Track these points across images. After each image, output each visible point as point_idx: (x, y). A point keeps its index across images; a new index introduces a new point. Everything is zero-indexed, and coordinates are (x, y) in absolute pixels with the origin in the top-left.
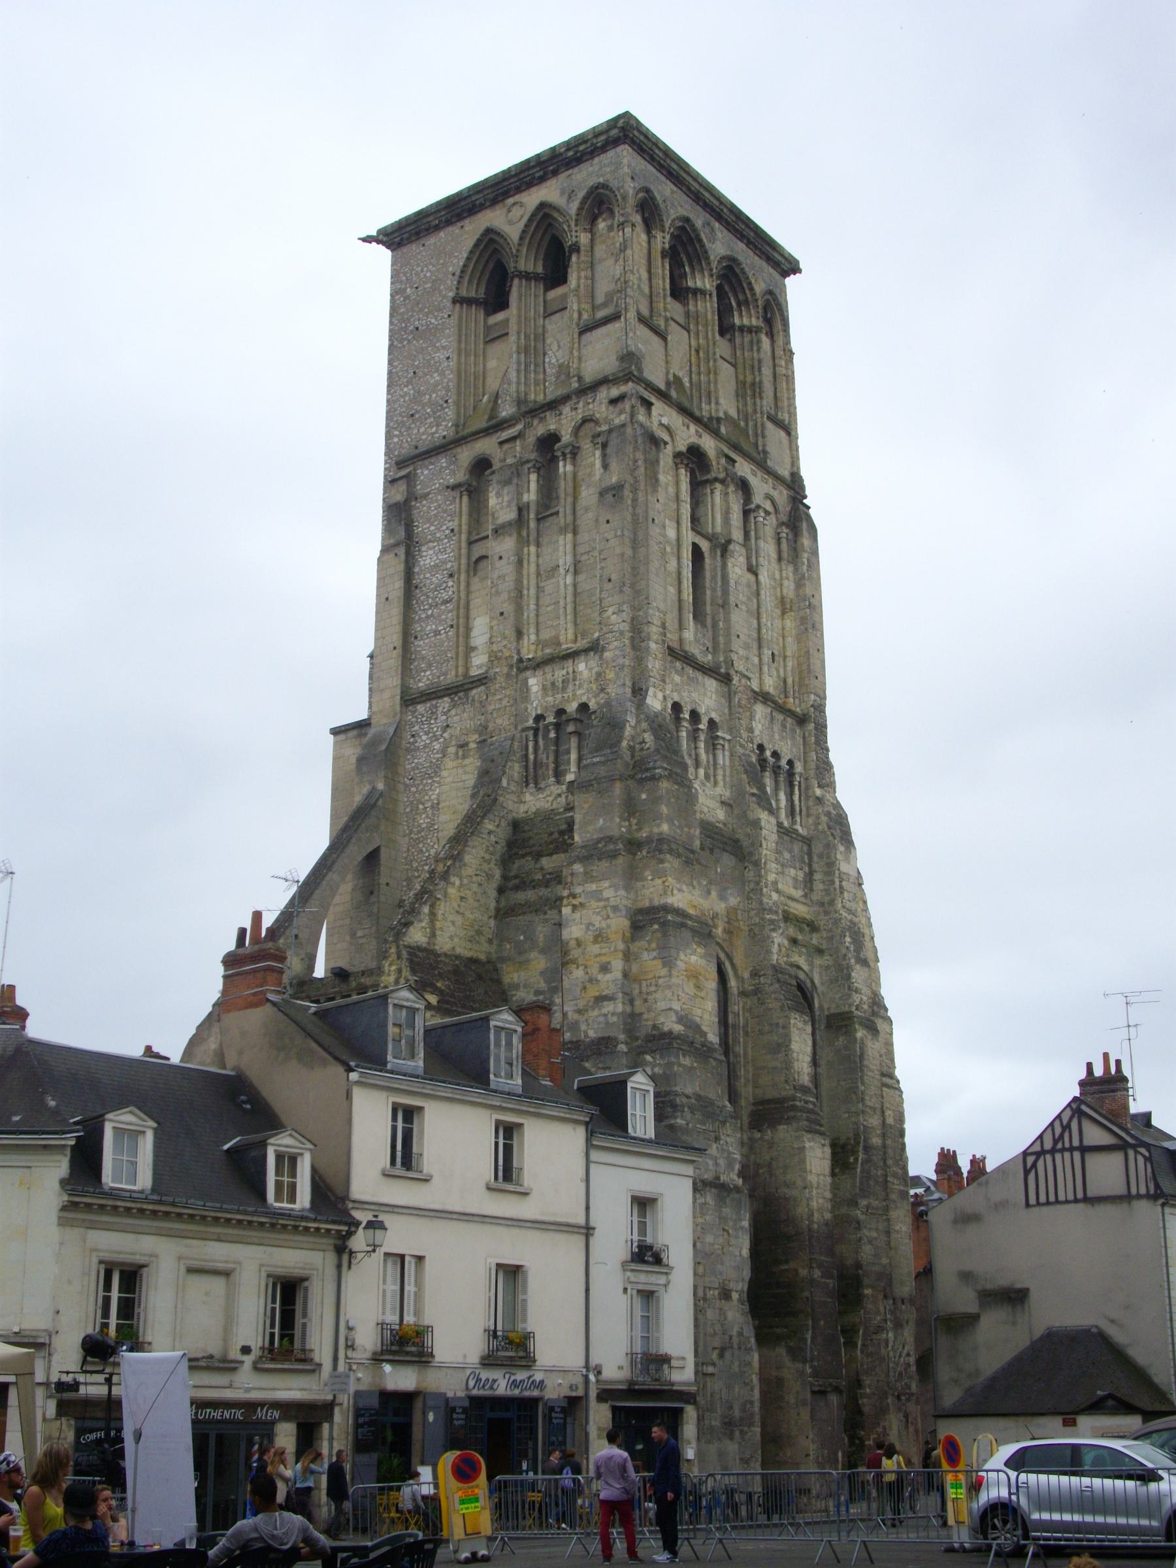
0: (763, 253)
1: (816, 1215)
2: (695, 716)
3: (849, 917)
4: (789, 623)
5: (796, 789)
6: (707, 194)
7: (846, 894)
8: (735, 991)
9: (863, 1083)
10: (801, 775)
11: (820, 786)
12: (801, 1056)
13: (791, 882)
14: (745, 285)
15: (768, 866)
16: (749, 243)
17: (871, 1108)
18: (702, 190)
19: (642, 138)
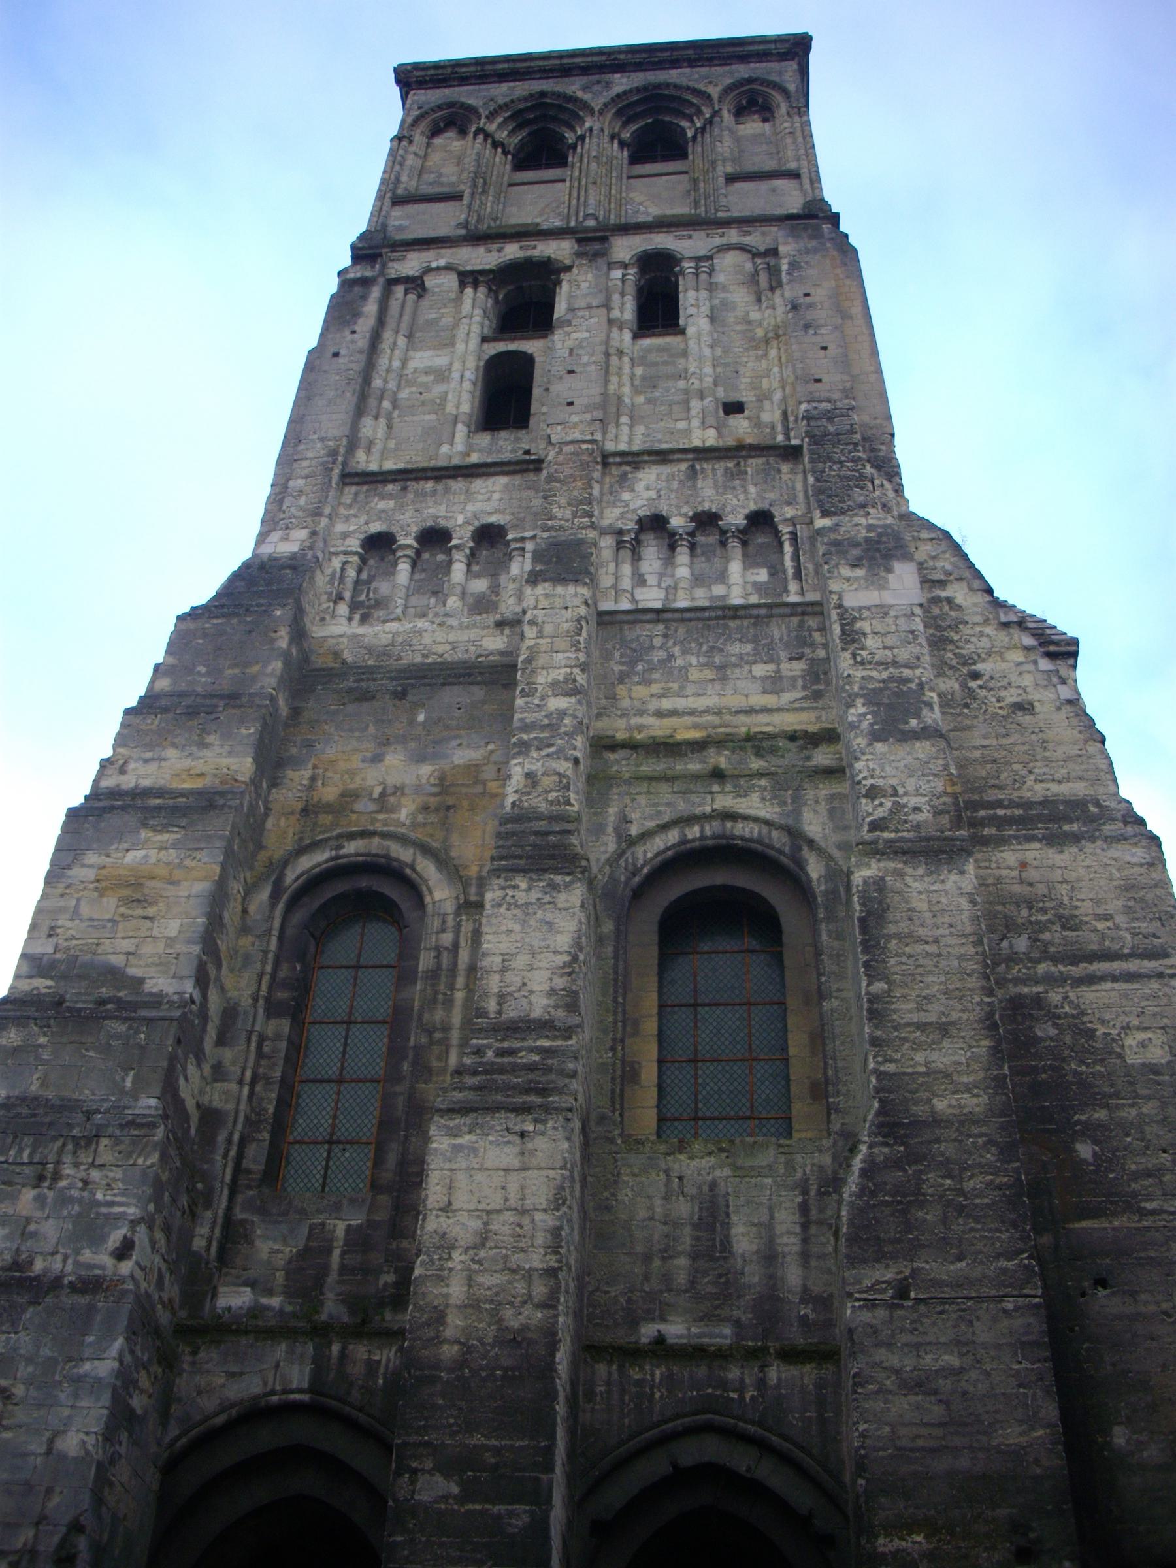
0: (729, 58)
1: (455, 1323)
2: (435, 538)
3: (885, 675)
4: (773, 353)
5: (788, 549)
6: (577, 60)
7: (870, 642)
8: (449, 907)
9: (874, 970)
10: (792, 521)
11: (825, 514)
12: (521, 961)
13: (758, 686)
14: (689, 97)
15: (541, 660)
16: (692, 63)
17: (922, 1027)
18: (565, 61)
19: (432, 72)
